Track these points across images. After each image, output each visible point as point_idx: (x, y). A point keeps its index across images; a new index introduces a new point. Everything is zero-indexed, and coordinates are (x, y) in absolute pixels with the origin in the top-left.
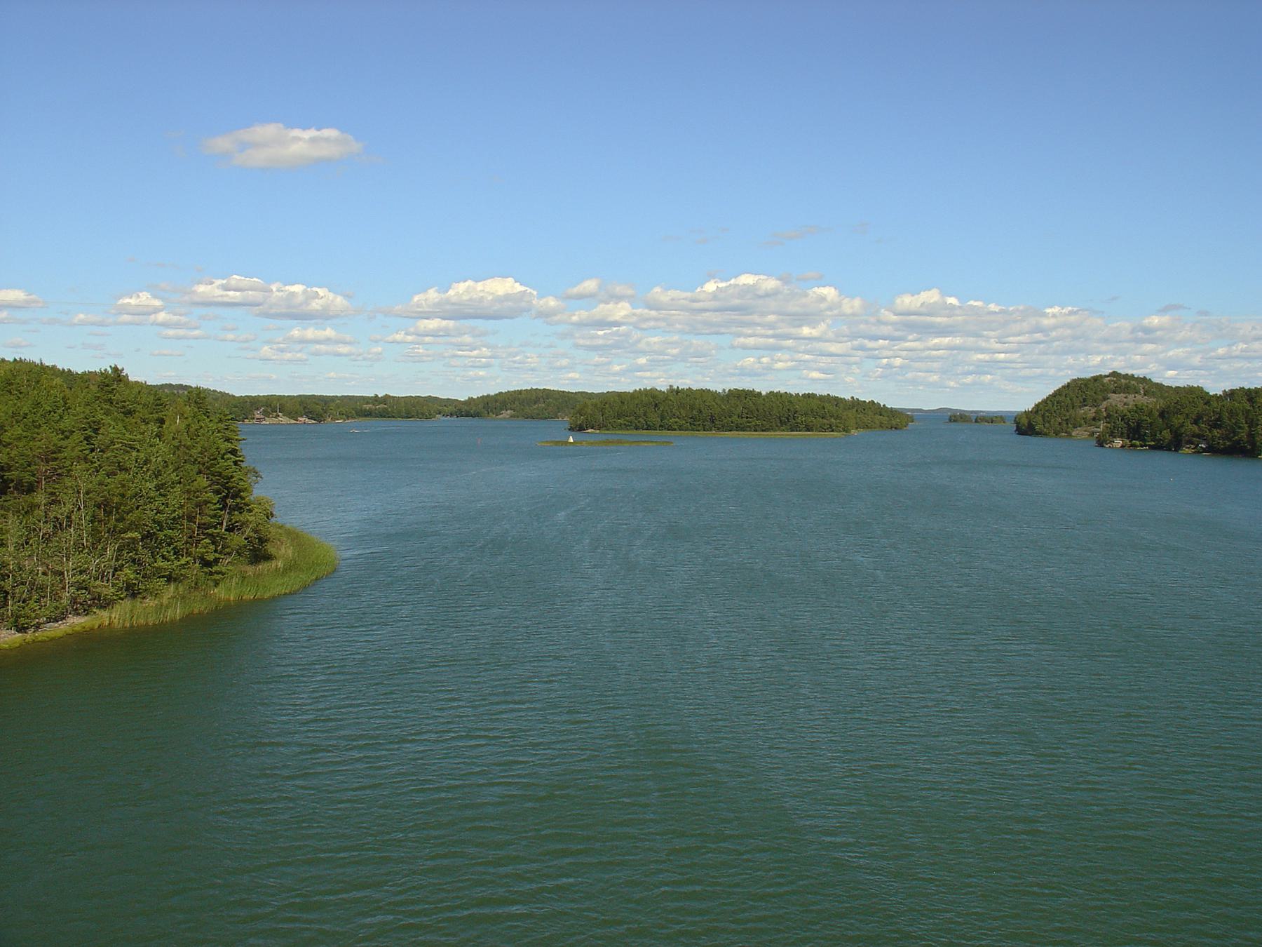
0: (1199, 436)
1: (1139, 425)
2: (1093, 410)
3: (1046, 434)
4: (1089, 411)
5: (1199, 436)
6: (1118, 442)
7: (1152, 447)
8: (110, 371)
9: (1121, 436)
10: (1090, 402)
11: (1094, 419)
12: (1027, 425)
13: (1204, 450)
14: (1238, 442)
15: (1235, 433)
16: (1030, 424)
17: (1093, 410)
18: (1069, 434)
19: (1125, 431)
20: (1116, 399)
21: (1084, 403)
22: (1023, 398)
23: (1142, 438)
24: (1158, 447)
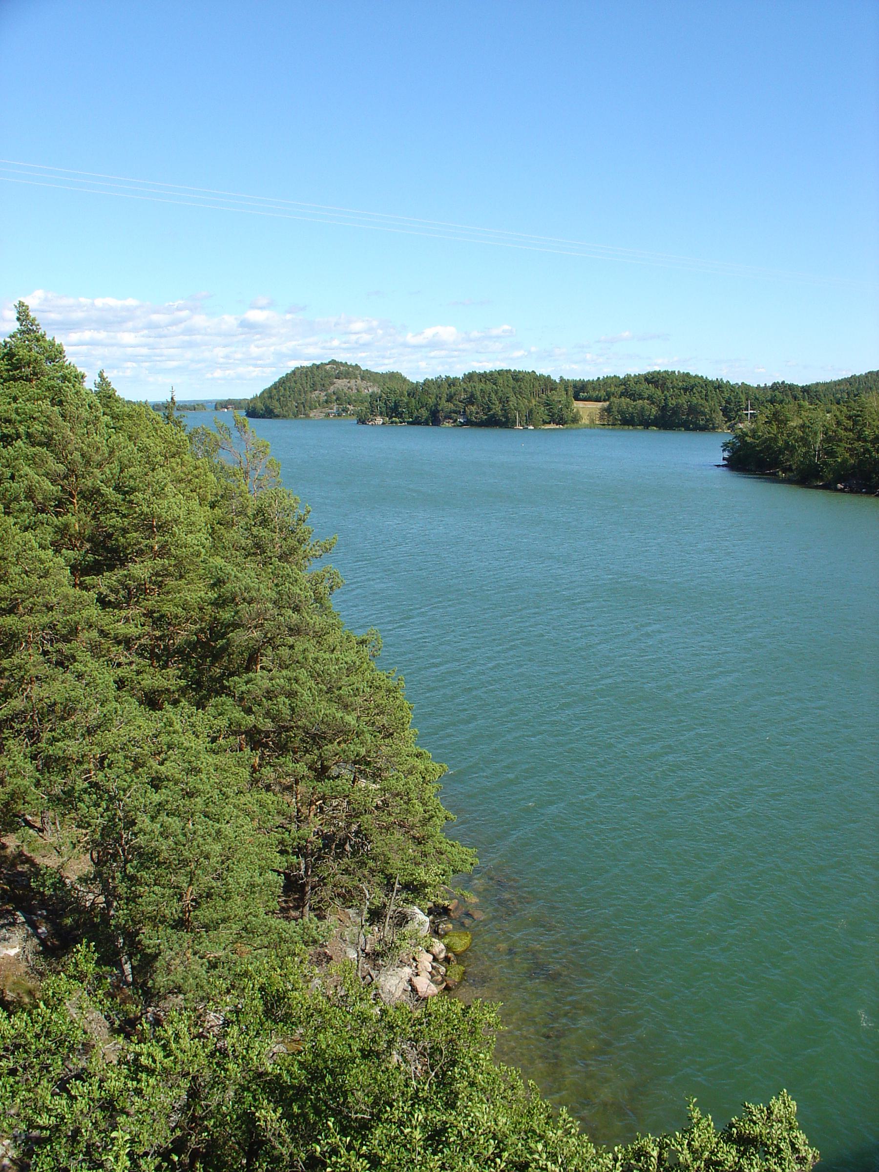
0: (455, 412)
1: (396, 405)
2: (323, 394)
3: (284, 417)
4: (319, 395)
5: (455, 412)
6: (379, 420)
7: (409, 423)
8: (90, 384)
9: (381, 414)
10: (319, 387)
11: (326, 402)
12: (261, 409)
13: (462, 424)
14: (493, 416)
15: (490, 409)
16: (267, 408)
17: (323, 394)
18: (307, 416)
19: (384, 409)
20: (341, 384)
21: (314, 388)
22: (251, 386)
23: (400, 415)
24: (416, 422)
